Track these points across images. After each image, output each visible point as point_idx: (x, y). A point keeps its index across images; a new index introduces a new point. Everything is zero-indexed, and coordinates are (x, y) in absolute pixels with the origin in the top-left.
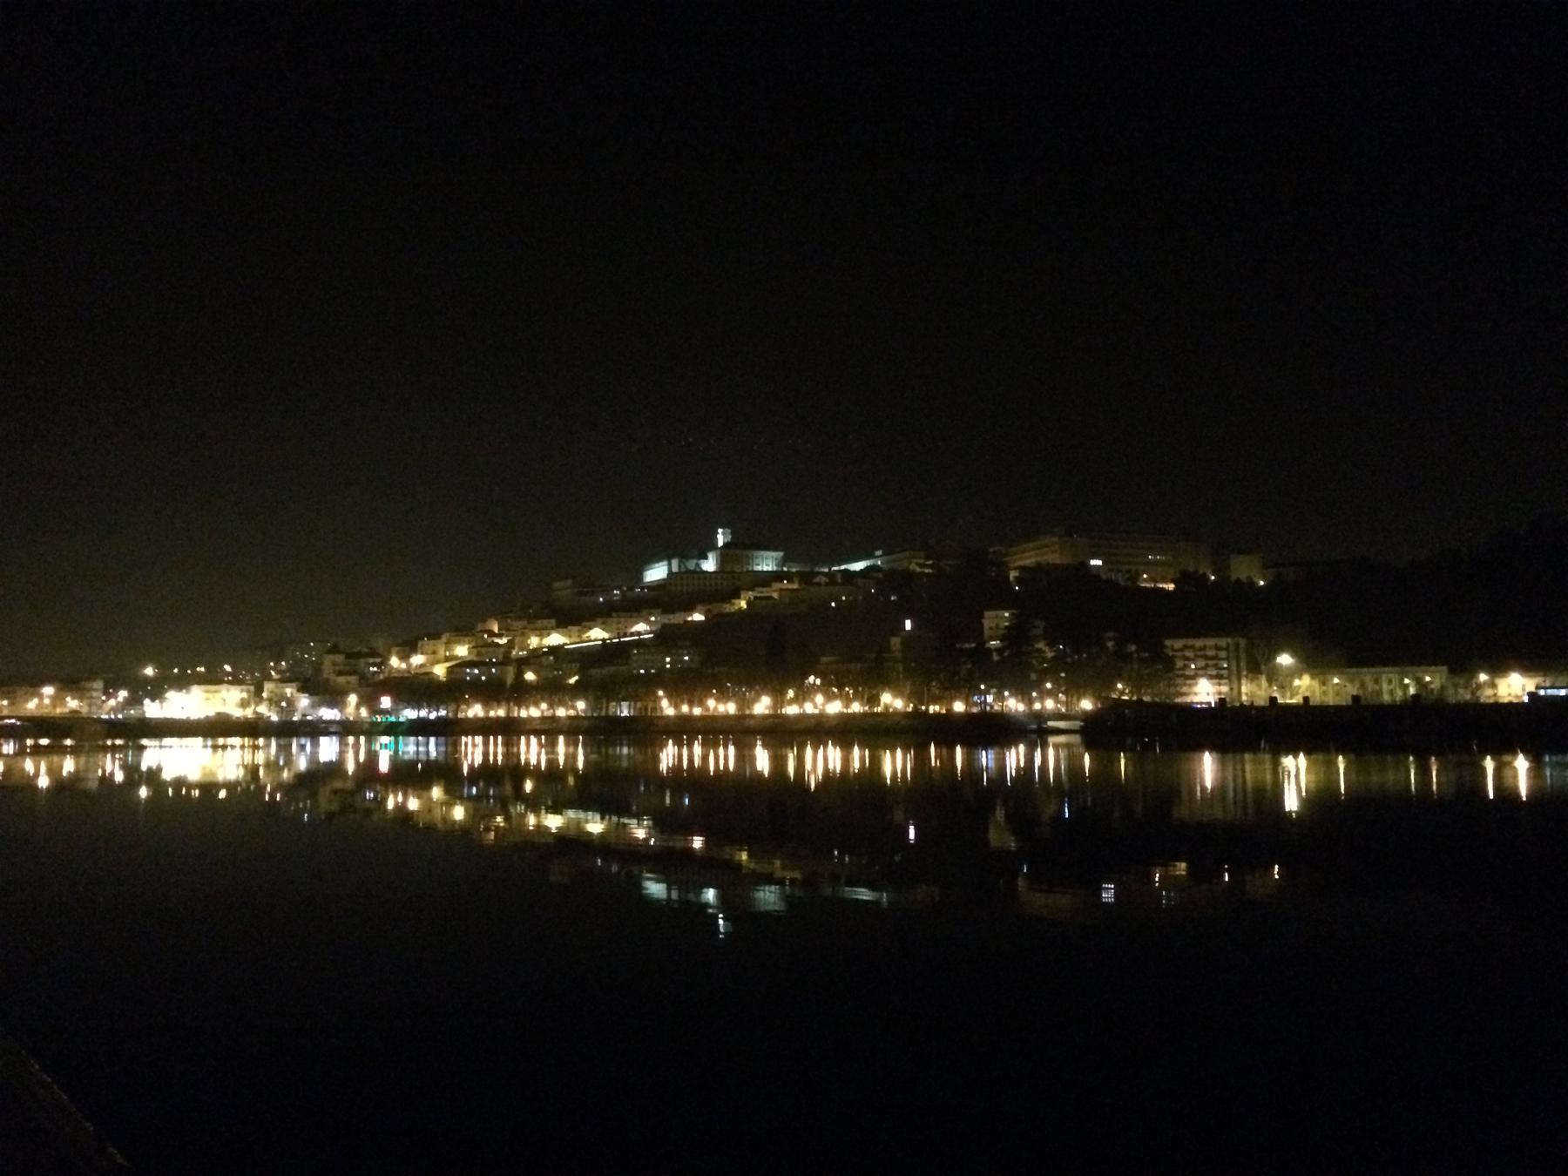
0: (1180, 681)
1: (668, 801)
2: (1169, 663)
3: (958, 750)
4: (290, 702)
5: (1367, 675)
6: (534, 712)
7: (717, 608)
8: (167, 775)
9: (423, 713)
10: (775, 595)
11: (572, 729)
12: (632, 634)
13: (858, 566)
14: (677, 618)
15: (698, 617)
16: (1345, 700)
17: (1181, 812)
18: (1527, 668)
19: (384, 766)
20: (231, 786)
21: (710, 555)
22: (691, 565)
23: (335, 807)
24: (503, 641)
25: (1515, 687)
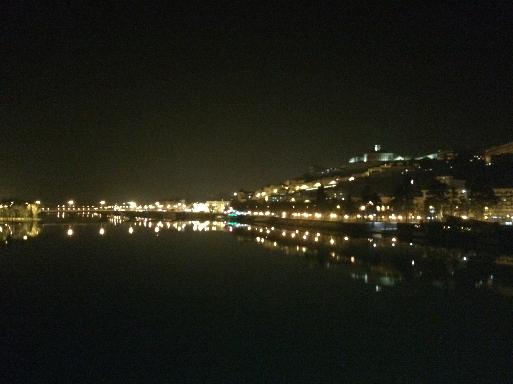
7: (358, 175)
10: (381, 170)
14: (345, 179)
15: (352, 179)
24: (287, 188)
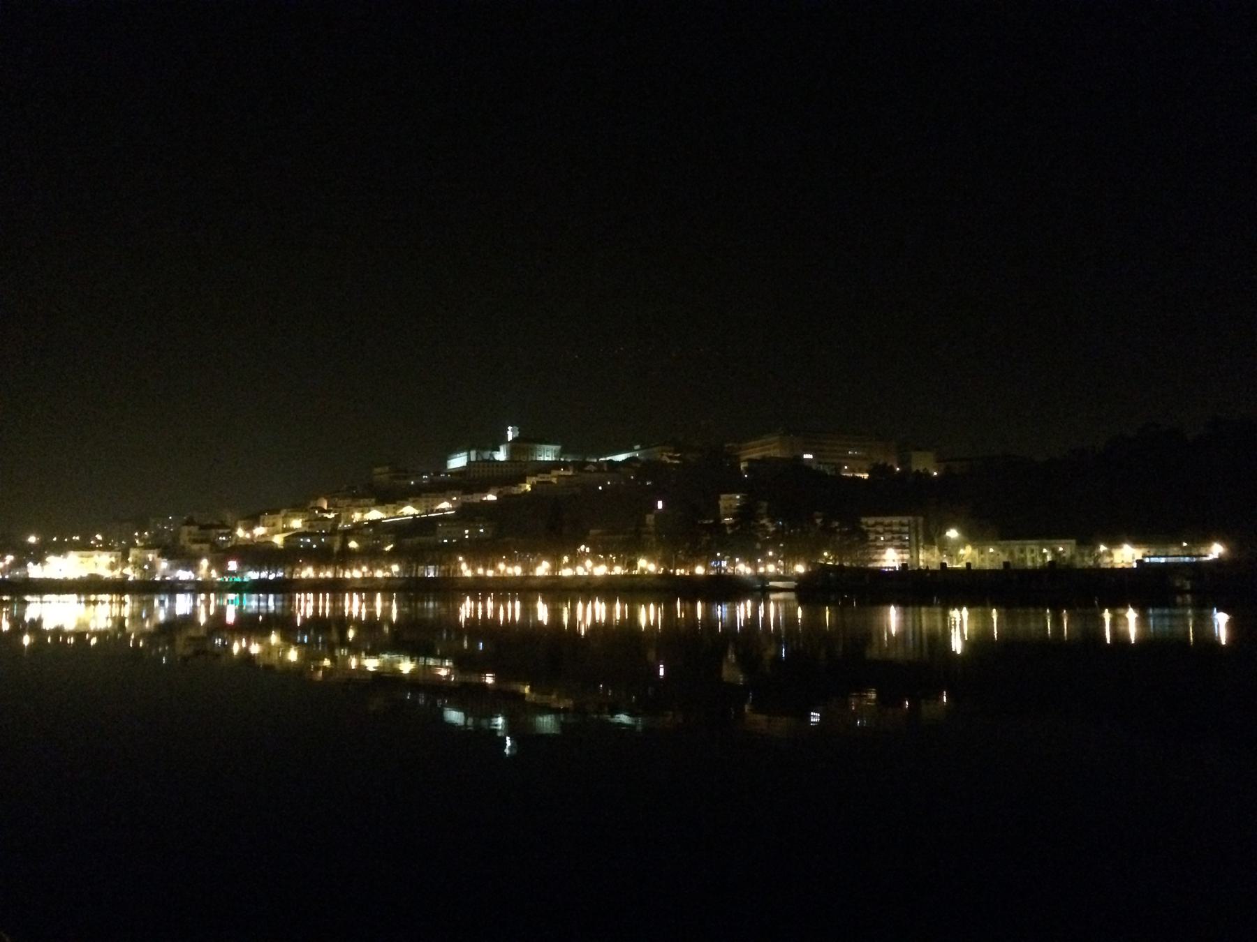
0: (873, 550)
1: (466, 645)
2: (864, 536)
3: (699, 606)
4: (152, 566)
5: (1016, 545)
6: (357, 574)
8: (48, 625)
9: (264, 575)
10: (554, 480)
11: (387, 588)
12: (438, 511)
13: (620, 458)
14: (475, 498)
15: (491, 497)
16: (998, 565)
17: (873, 653)
18: (1136, 542)
19: (231, 618)
20: (100, 634)
21: (502, 448)
22: (486, 455)
23: (189, 651)
24: (332, 516)
25: (1126, 556)
